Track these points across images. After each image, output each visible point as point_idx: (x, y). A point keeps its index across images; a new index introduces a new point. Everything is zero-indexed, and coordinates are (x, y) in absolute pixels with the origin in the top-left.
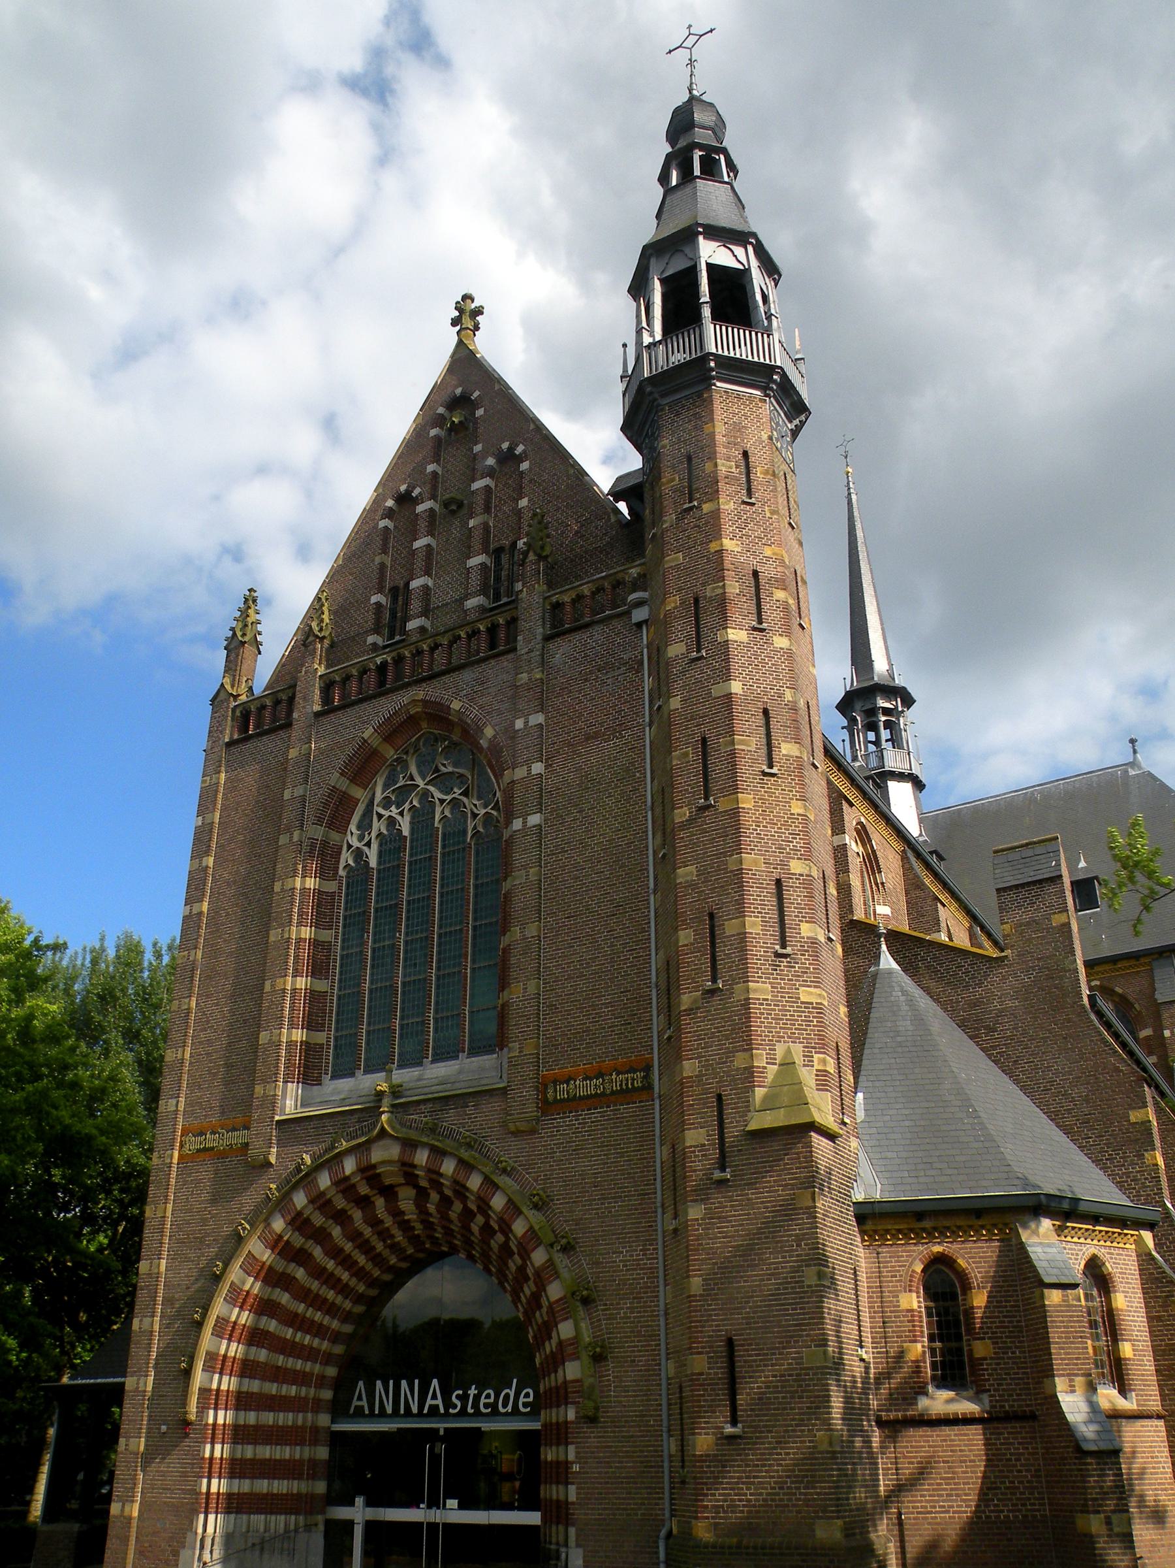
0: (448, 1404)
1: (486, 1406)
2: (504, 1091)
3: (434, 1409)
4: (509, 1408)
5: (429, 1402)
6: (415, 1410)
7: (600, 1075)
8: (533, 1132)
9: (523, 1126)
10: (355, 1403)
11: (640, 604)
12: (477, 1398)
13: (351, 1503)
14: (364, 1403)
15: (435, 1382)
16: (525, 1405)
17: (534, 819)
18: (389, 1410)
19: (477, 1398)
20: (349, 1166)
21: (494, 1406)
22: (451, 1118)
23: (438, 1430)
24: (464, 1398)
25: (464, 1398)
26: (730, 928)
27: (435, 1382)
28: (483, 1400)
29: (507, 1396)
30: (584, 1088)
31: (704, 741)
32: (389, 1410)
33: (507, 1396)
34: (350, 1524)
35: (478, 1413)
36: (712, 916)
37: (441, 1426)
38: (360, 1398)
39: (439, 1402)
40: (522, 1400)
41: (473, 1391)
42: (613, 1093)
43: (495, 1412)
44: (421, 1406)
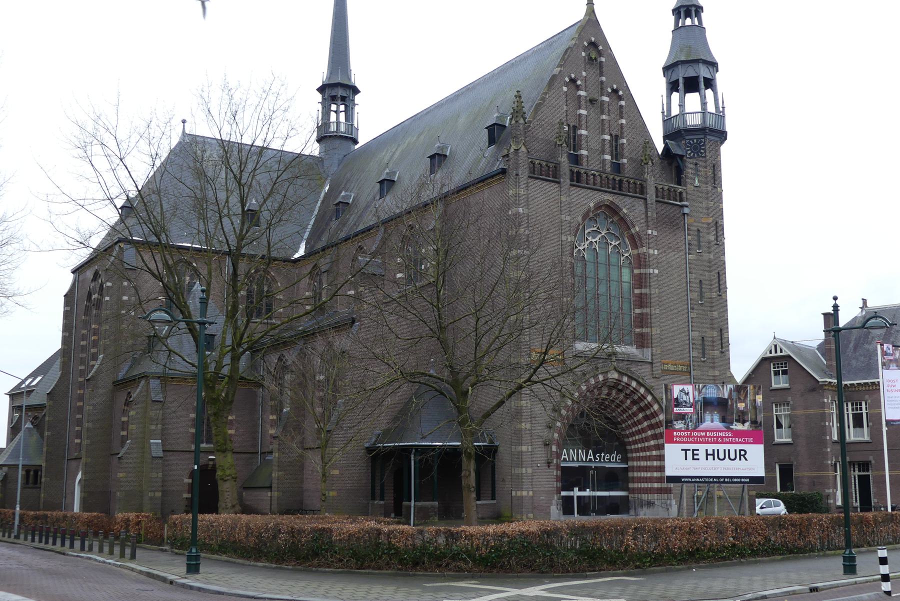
0: (595, 458)
1: (607, 459)
2: (651, 363)
3: (590, 460)
4: (614, 460)
5: (589, 457)
6: (584, 460)
7: (676, 365)
8: (659, 378)
9: (657, 376)
10: (563, 457)
11: (687, 206)
12: (604, 457)
13: (573, 490)
14: (566, 457)
15: (590, 451)
16: (619, 459)
17: (656, 271)
18: (575, 460)
19: (604, 457)
20: (601, 378)
21: (610, 459)
22: (633, 368)
23: (592, 466)
24: (600, 457)
25: (600, 457)
26: (725, 335)
27: (590, 451)
28: (606, 458)
29: (613, 456)
30: (672, 368)
31: (719, 273)
32: (575, 460)
33: (613, 456)
34: (573, 497)
35: (604, 461)
36: (721, 330)
37: (593, 465)
38: (590, 456)
39: (592, 457)
40: (618, 458)
41: (603, 455)
42: (679, 371)
43: (610, 461)
44: (586, 459)
